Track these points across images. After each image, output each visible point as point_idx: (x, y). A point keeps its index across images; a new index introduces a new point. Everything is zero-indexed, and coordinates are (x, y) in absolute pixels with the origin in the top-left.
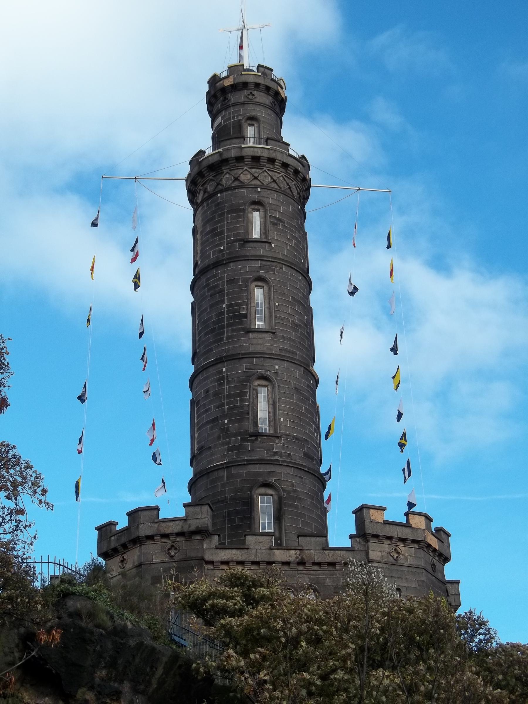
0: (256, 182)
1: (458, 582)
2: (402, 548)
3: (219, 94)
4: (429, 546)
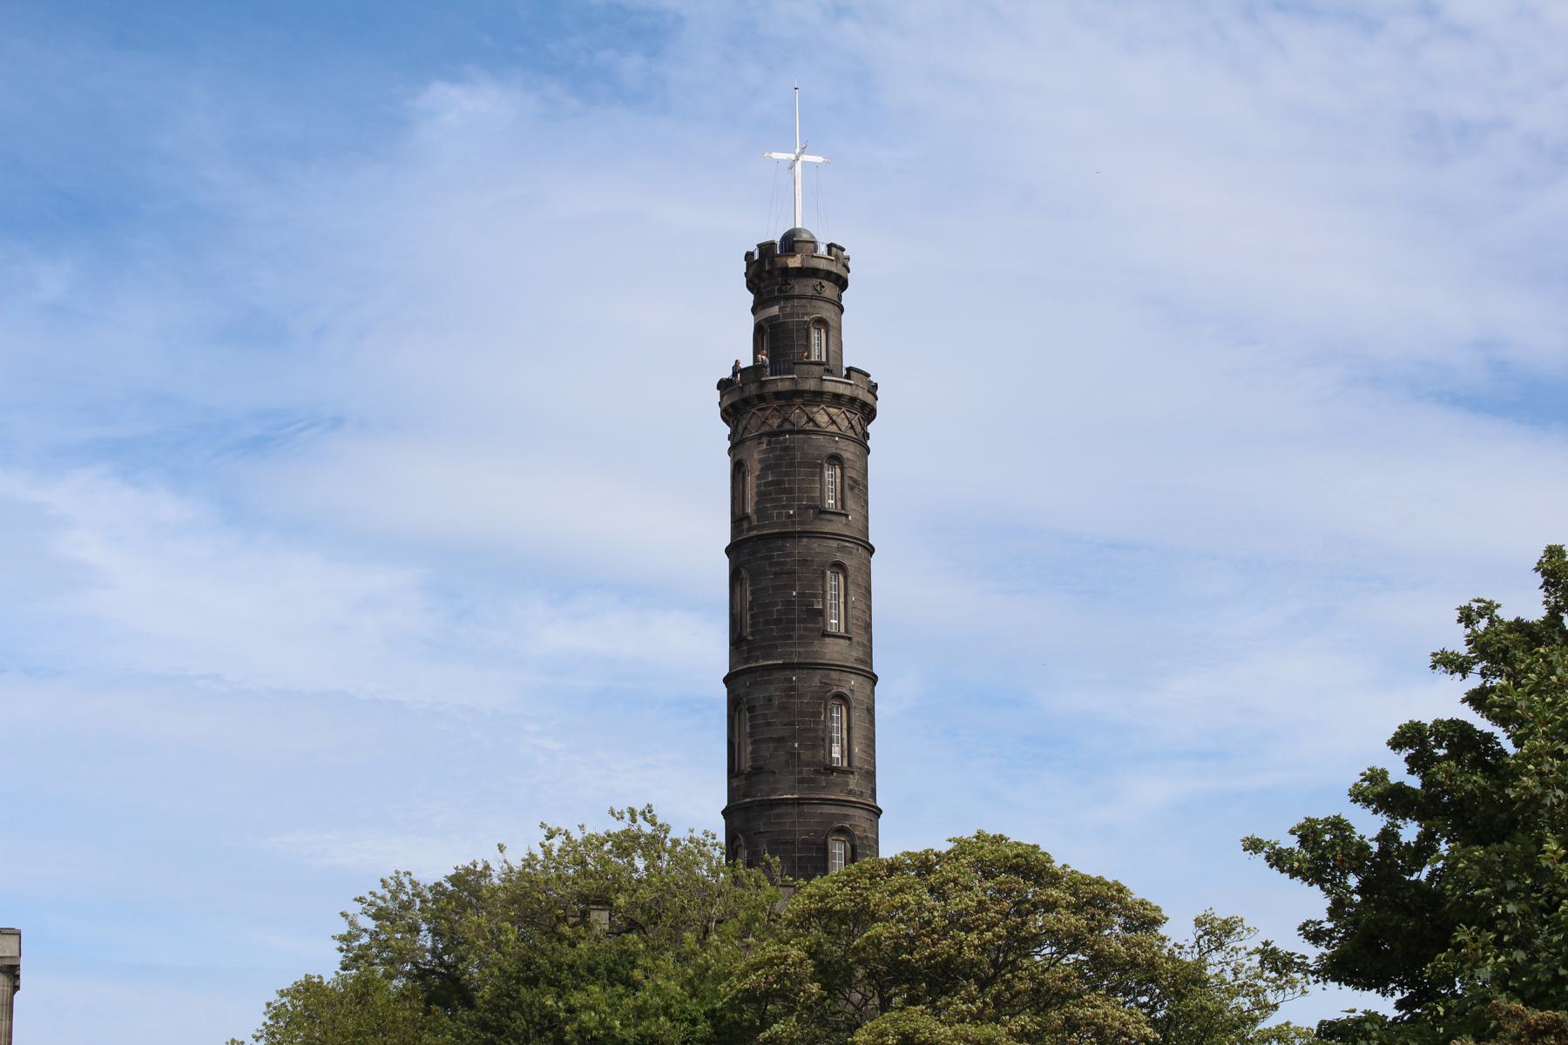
0: (833, 428)
3: (777, 273)
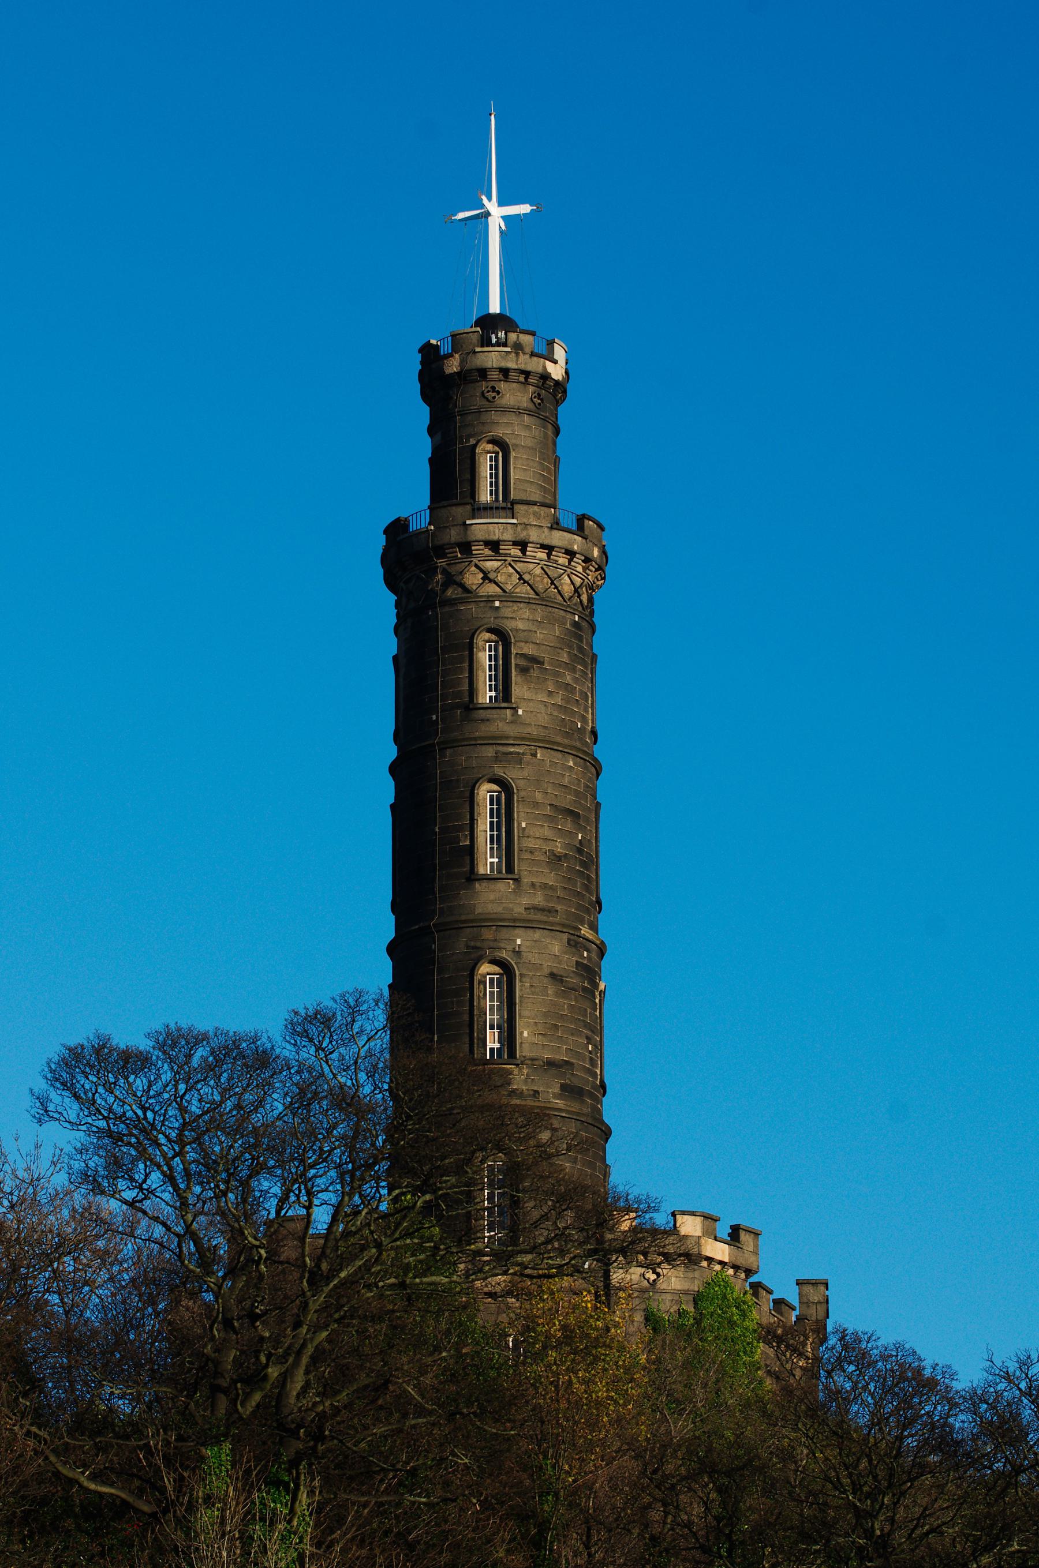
0: (491, 589)
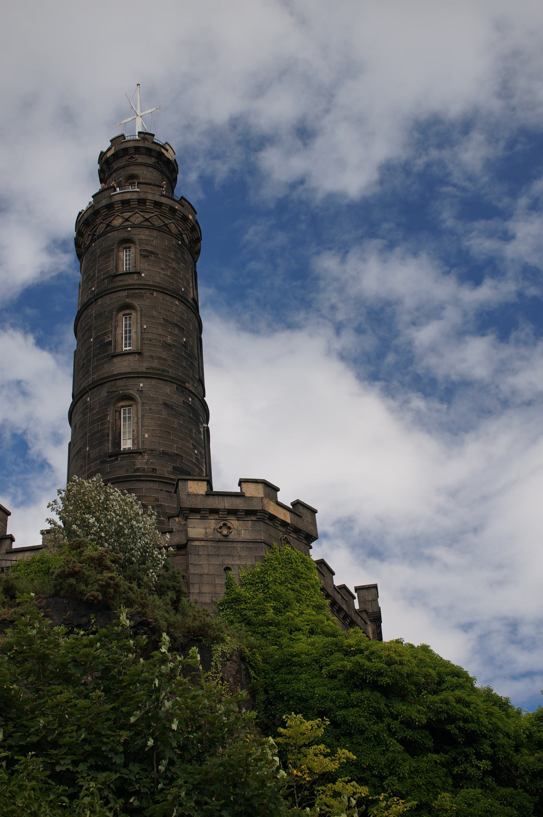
1: (375, 587)
2: (234, 523)
4: (272, 518)
